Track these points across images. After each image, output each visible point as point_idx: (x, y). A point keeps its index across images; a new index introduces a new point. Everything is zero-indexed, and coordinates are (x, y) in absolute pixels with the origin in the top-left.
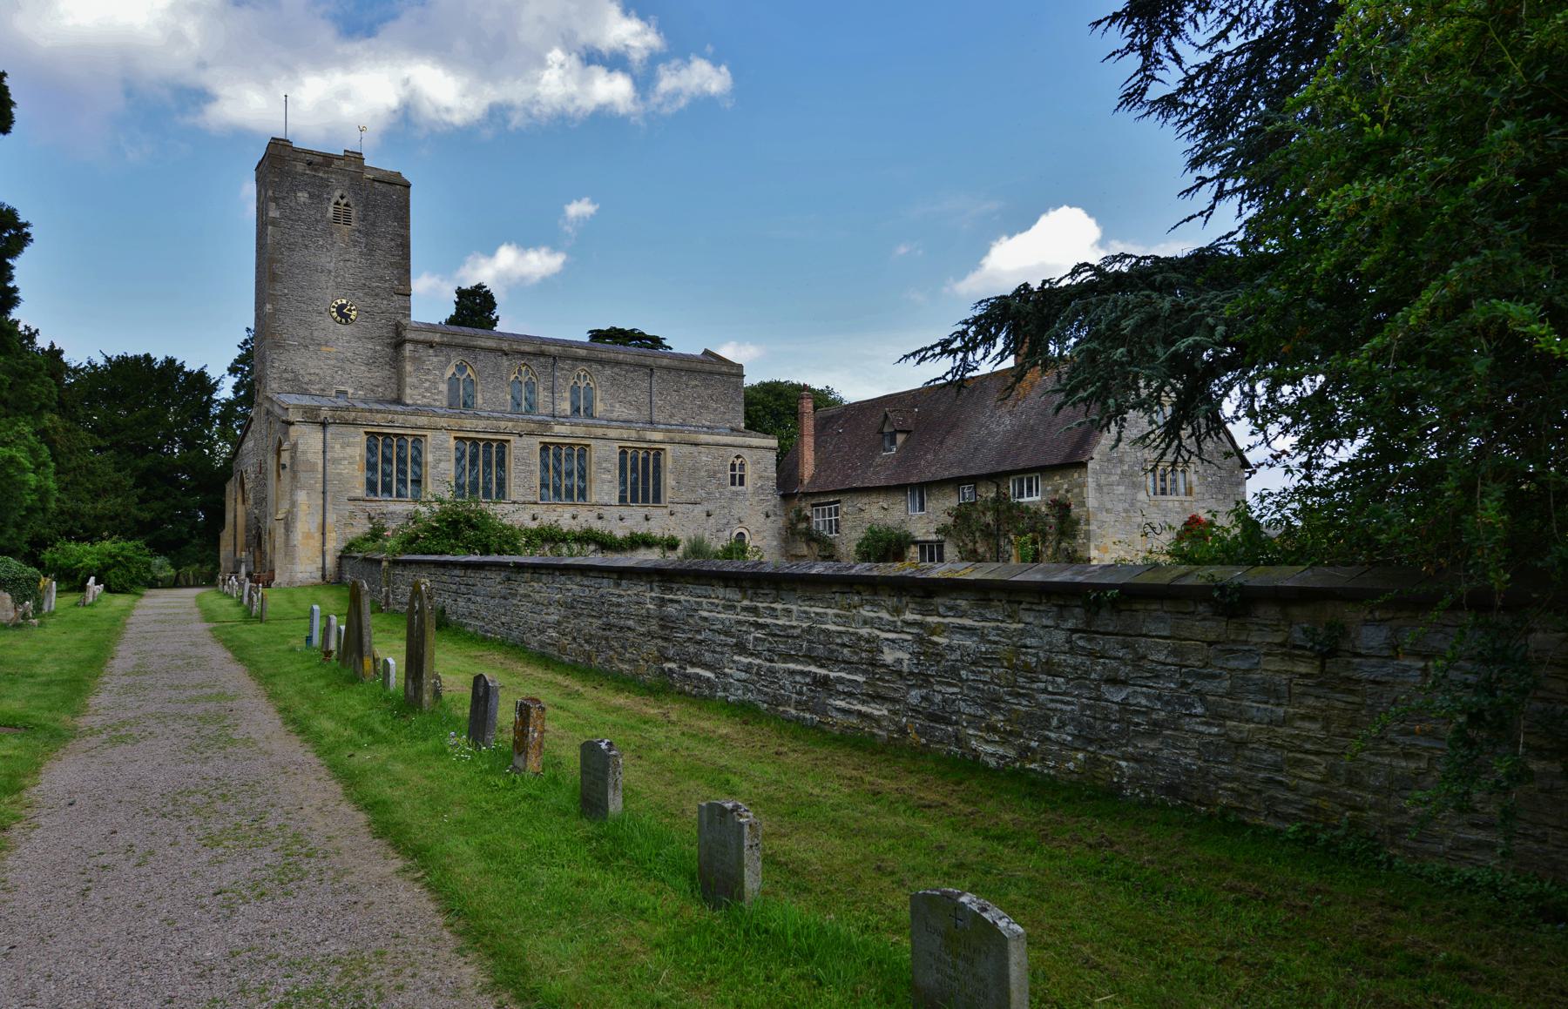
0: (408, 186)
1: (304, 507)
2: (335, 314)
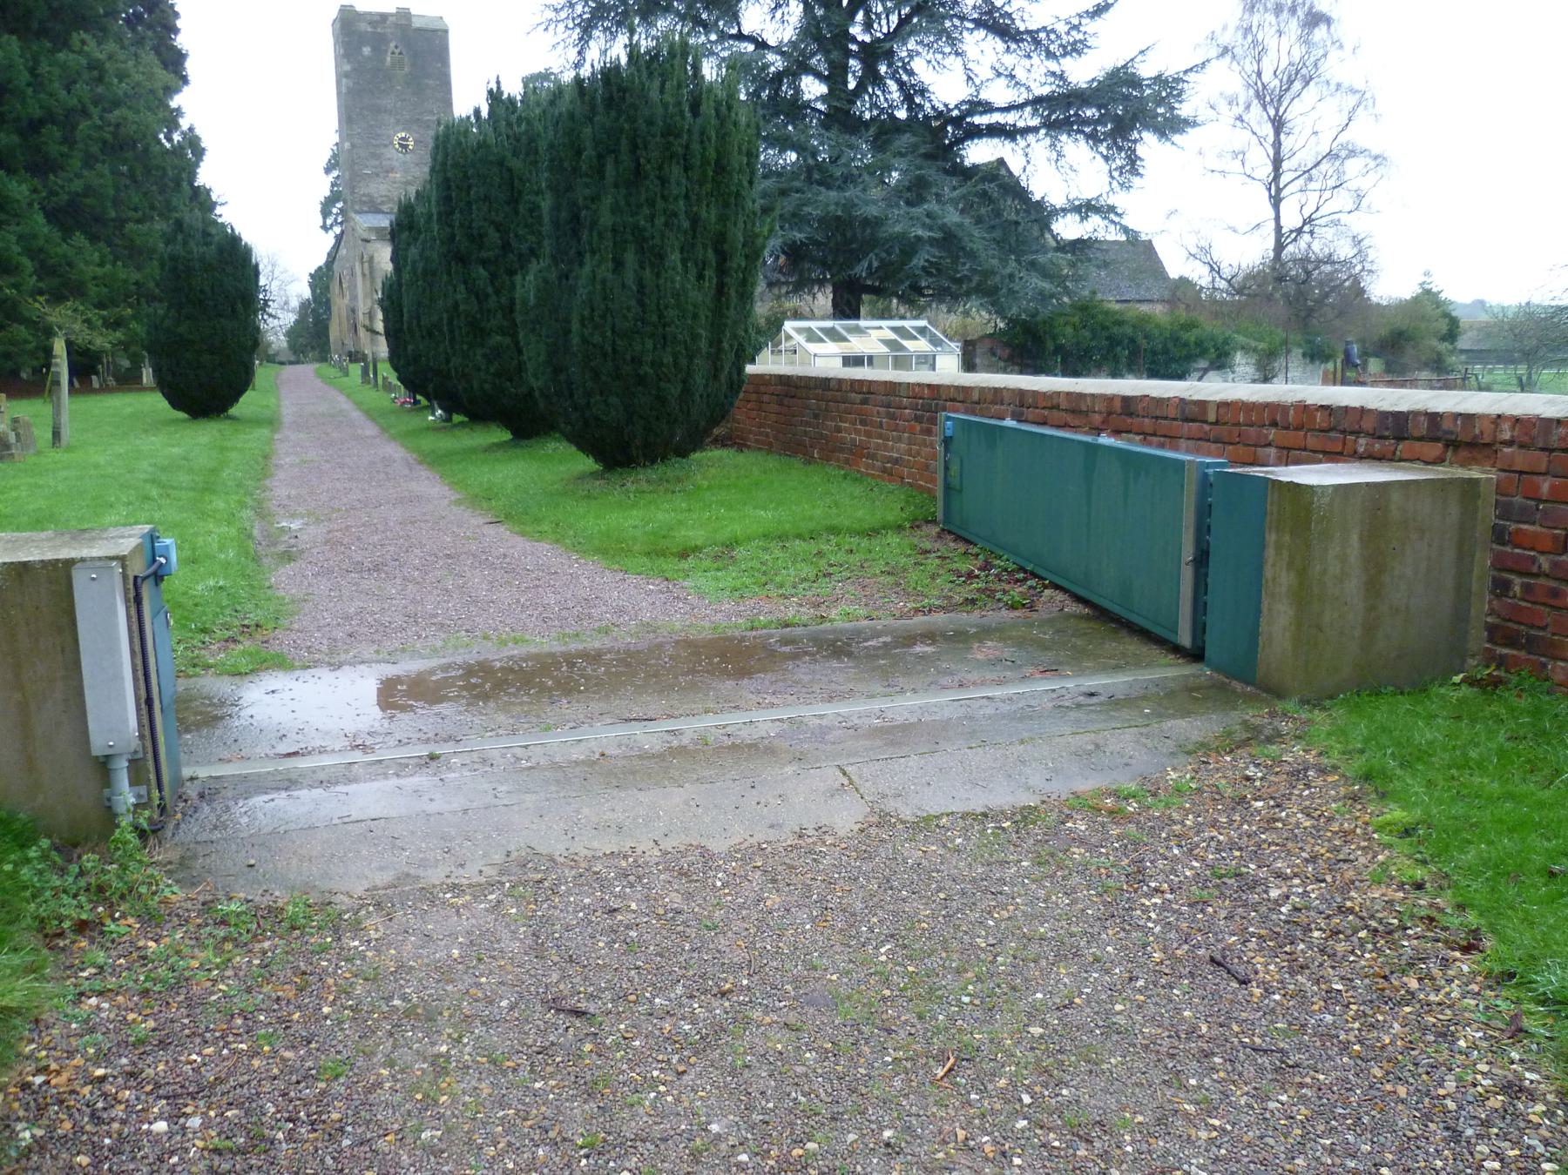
0: (446, 31)
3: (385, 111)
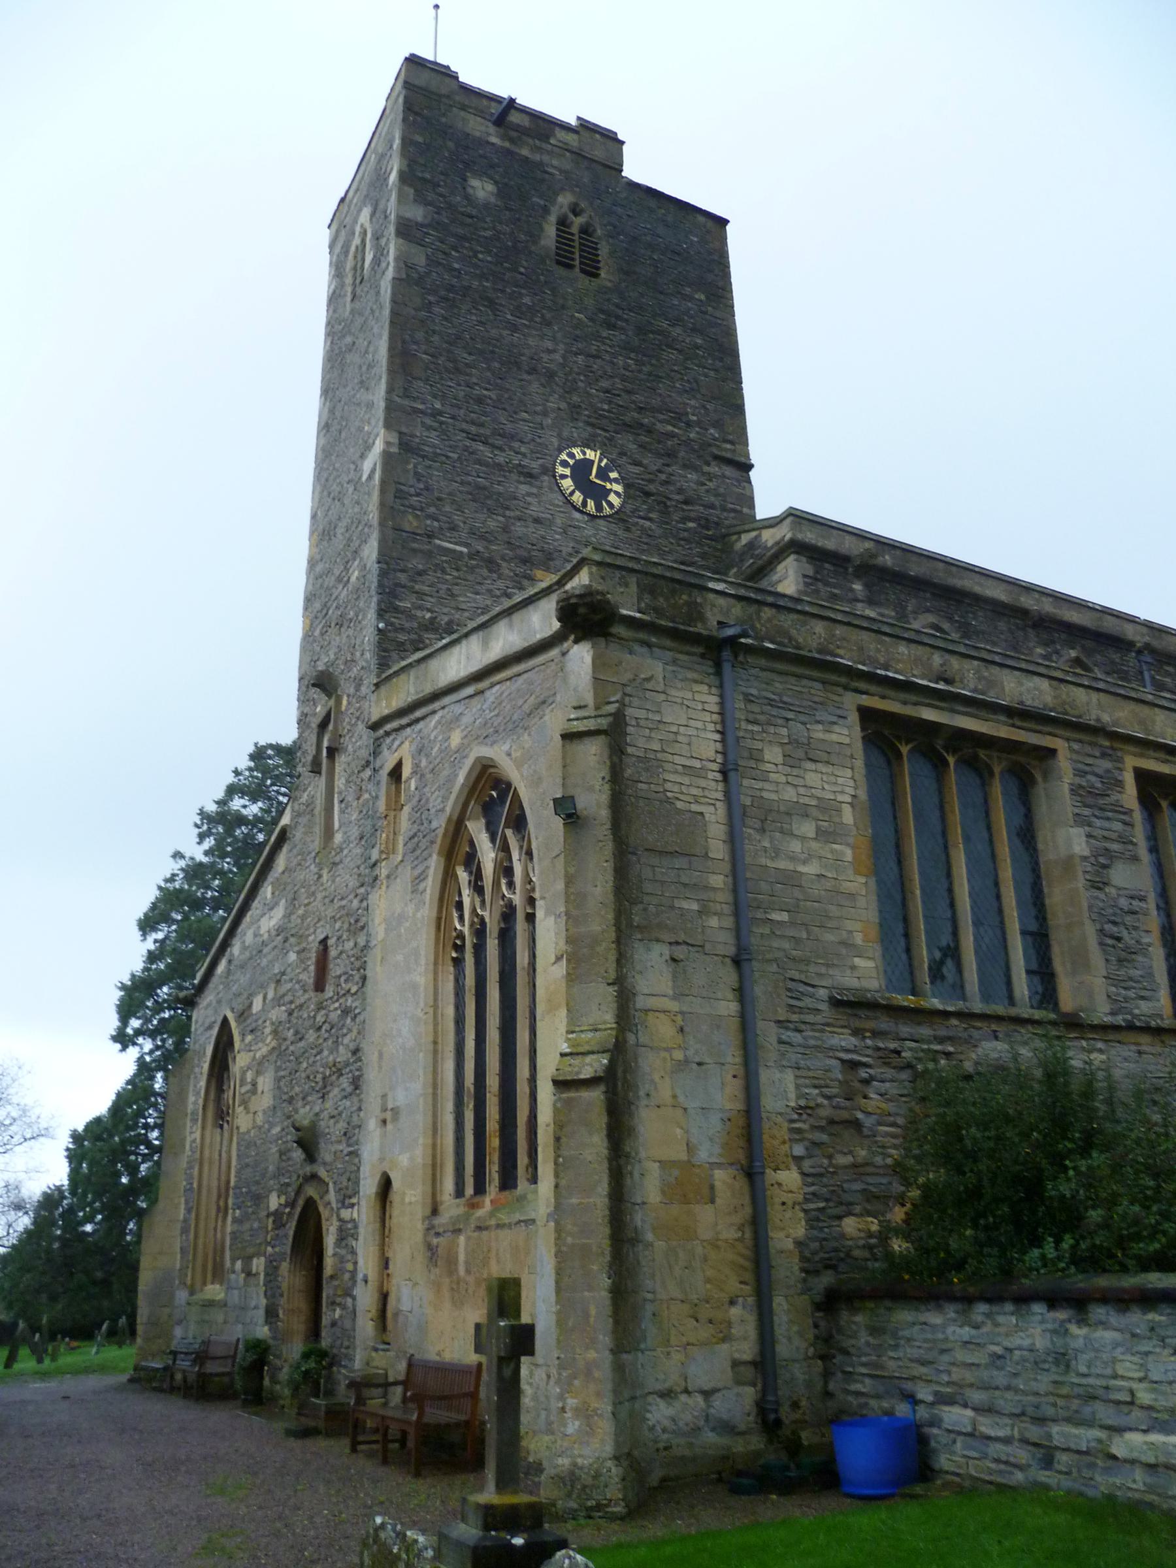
0: (723, 222)
1: (663, 1029)
2: (568, 484)
3: (532, 371)
